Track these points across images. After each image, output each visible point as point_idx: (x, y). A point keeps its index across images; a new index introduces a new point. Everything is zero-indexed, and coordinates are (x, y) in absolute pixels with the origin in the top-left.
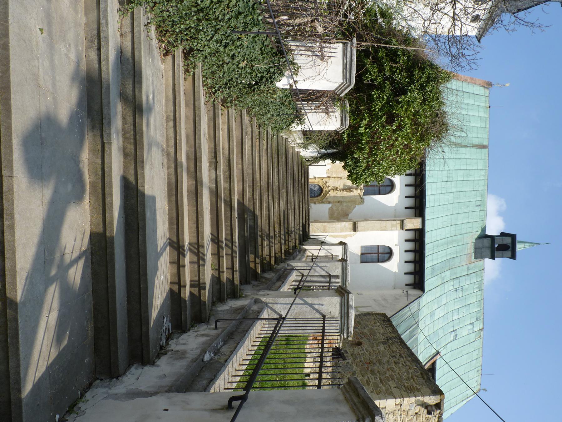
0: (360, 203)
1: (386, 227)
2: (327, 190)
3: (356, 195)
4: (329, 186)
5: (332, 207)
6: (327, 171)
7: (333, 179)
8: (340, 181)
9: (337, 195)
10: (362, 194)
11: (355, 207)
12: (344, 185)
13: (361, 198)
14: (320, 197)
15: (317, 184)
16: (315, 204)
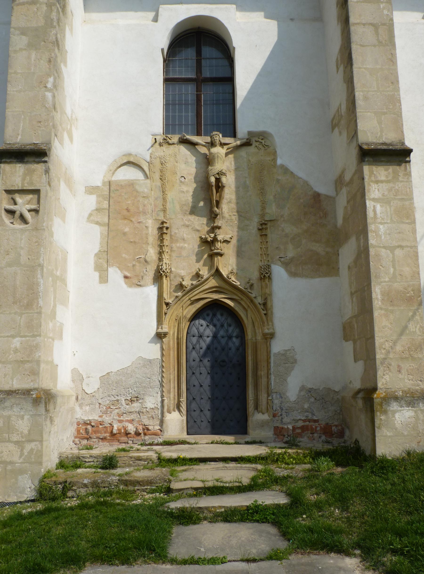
0: (266, 146)
1: (375, 27)
2: (213, 283)
3: (233, 167)
4: (198, 275)
5: (286, 265)
7: (166, 257)
8: (174, 230)
9: (234, 242)
10: (227, 140)
11: (285, 170)
12: (194, 211)
13: (247, 144)
15: (185, 325)
16: (272, 336)
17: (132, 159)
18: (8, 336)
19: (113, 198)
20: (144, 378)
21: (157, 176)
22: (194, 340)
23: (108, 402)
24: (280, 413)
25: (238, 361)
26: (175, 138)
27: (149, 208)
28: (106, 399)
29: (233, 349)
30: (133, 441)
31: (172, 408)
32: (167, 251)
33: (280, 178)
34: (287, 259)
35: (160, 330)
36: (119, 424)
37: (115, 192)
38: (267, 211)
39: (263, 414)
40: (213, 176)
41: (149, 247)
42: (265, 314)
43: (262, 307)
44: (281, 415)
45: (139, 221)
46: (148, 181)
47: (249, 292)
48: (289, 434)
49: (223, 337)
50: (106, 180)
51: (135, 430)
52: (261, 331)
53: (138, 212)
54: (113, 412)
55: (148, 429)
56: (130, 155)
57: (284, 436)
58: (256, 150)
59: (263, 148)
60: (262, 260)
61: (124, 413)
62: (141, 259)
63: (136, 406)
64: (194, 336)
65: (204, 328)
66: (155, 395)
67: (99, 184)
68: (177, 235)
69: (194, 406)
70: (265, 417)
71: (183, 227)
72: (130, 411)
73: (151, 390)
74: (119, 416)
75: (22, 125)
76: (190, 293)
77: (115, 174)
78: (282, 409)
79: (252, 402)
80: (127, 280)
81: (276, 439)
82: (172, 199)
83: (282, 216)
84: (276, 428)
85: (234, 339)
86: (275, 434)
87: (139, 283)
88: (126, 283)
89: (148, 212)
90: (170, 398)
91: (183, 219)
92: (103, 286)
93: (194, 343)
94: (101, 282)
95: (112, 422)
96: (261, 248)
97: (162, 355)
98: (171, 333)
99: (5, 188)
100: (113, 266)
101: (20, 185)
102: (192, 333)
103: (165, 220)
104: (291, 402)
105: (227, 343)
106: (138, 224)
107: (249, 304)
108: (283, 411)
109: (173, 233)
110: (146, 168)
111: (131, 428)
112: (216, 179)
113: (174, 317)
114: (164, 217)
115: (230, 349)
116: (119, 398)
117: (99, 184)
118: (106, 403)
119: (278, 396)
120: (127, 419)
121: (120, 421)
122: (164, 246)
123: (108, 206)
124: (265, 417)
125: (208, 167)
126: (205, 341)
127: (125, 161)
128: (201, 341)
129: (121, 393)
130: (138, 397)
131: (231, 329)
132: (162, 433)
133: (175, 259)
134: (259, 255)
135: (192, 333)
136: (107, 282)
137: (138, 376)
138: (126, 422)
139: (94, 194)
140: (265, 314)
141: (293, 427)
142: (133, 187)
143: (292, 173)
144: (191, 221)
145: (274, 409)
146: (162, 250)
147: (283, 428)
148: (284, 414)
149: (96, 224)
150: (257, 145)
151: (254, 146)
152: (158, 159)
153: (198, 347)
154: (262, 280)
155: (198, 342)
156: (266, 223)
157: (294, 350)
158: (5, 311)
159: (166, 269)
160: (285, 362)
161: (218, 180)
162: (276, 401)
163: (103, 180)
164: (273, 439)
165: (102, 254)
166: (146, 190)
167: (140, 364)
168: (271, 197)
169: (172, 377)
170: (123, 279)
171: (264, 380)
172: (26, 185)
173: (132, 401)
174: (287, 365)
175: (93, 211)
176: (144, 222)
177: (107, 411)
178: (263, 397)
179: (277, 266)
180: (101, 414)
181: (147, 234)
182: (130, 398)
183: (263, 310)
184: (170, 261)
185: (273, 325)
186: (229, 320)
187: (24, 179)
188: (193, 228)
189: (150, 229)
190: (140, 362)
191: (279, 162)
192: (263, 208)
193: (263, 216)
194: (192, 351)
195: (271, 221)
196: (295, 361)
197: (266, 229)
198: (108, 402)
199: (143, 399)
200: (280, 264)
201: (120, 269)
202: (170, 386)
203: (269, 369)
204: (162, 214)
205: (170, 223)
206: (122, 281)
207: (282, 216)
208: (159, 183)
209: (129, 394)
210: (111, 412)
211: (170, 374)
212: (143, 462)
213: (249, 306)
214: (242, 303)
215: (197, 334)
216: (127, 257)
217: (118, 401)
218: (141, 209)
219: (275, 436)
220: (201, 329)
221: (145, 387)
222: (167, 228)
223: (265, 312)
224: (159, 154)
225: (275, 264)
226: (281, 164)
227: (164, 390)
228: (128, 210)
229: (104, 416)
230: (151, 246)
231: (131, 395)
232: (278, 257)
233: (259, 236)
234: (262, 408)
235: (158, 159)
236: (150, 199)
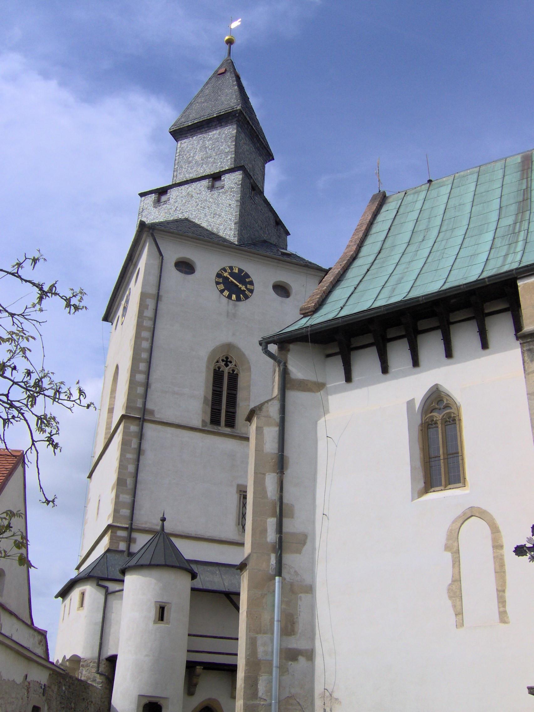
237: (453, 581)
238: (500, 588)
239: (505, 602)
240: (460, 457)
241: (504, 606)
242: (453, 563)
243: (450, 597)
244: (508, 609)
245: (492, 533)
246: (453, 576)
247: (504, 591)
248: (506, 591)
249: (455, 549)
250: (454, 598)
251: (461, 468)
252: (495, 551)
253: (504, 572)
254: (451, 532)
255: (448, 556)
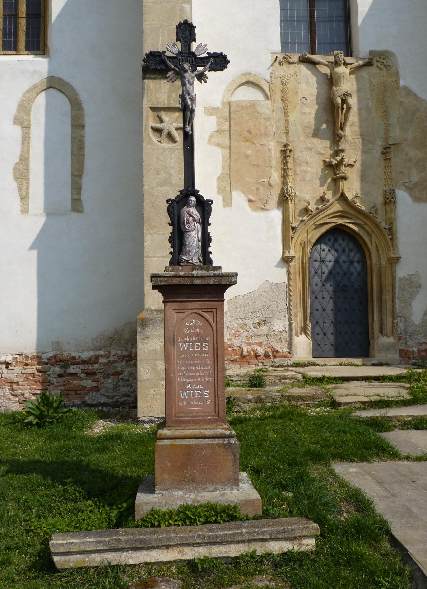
2: (337, 207)
3: (355, 88)
4: (322, 200)
5: (410, 189)
6: (255, 209)
7: (290, 181)
8: (297, 153)
9: (358, 166)
11: (408, 92)
12: (316, 134)
13: (369, 64)
14: (366, 239)
15: (308, 249)
16: (398, 259)
17: (251, 79)
18: (163, 256)
19: (234, 119)
20: (271, 302)
21: (278, 97)
22: (317, 264)
23: (236, 325)
24: (404, 337)
25: (360, 286)
26: (295, 58)
27: (271, 130)
28: (234, 323)
29: (355, 274)
30: (263, 363)
31: (299, 332)
32: (290, 174)
33: (403, 100)
34: (411, 184)
35: (287, 254)
36: (248, 347)
37: (235, 112)
38: (391, 134)
39: (388, 337)
40: (340, 96)
41: (272, 170)
42: (390, 239)
43: (388, 232)
44: (406, 338)
45: (262, 143)
46: (269, 102)
47: (375, 217)
48: (415, 357)
49: (344, 262)
50: (226, 100)
51: (264, 352)
52: (385, 256)
53: (260, 134)
54: (242, 335)
55: (277, 352)
56: (249, 74)
57: (410, 358)
58: (377, 71)
59: (384, 69)
60: (387, 184)
61: (253, 336)
62: (265, 183)
63: (264, 329)
64: (316, 261)
65: (325, 254)
66: (282, 319)
67: (219, 104)
68: (301, 158)
69: (317, 329)
70: (391, 340)
71: (306, 150)
72: (259, 334)
73: (278, 313)
74: (248, 338)
75: (161, 39)
76: (315, 217)
77: (234, 94)
78: (406, 333)
79: (377, 325)
80: (251, 204)
81: (402, 362)
82: (294, 121)
83: (406, 140)
84: (401, 351)
85: (356, 264)
86: (401, 356)
87: (263, 207)
88: (250, 207)
89: (270, 134)
90: (297, 322)
91: (305, 142)
92: (228, 210)
93: (317, 268)
94: (224, 206)
95: (241, 345)
96: (385, 172)
97: (289, 279)
98: (297, 257)
99: (150, 106)
100: (236, 189)
101: (166, 102)
102: (314, 258)
103: (288, 143)
104: (415, 325)
105: (348, 268)
106: (261, 146)
107: (373, 228)
108: (408, 335)
109: (296, 157)
110: (266, 88)
111: (261, 351)
112: (342, 100)
113: (299, 242)
114: (287, 139)
115: (352, 274)
116: (247, 321)
117: (219, 104)
118: (235, 327)
119: (403, 320)
120: (255, 341)
121: (249, 344)
122: (288, 169)
123: (228, 128)
124: (391, 340)
125: (331, 88)
126: (327, 266)
127: (245, 81)
128: (323, 266)
129: (249, 317)
130: (266, 321)
131: (352, 254)
132: (291, 355)
133: (299, 183)
134: (383, 179)
135: (314, 258)
136: (231, 205)
137: (264, 299)
138: (254, 345)
139: (214, 115)
140: (390, 239)
141: (418, 350)
142: (254, 108)
143: (415, 95)
144: (314, 144)
145: (399, 332)
146: (286, 173)
147: (408, 351)
148: (409, 338)
149: (217, 146)
150: (379, 65)
151: (375, 66)
152: (279, 79)
153: (320, 272)
154: (387, 205)
155: (320, 266)
156: (390, 146)
157: (418, 275)
158: (158, 231)
159: (292, 193)
160: (410, 287)
161: (344, 101)
162: (401, 325)
163: (222, 101)
164: (399, 361)
165: (225, 177)
166: (267, 111)
167: (267, 287)
168: (395, 120)
169: (298, 301)
170: (247, 203)
171: (389, 304)
172: (172, 102)
173: (259, 324)
174: (411, 289)
175: (213, 132)
176: (266, 144)
177: (235, 334)
178: (388, 321)
179: (401, 191)
180: (230, 337)
181: (270, 157)
182: (258, 321)
183: (389, 235)
184: (294, 185)
185: (397, 250)
186: (351, 245)
187: (169, 97)
188: (316, 151)
189: (273, 152)
190: (267, 286)
191: (402, 83)
192: (387, 131)
193: (386, 139)
194: (314, 276)
195: (394, 144)
196: (420, 286)
197: (390, 152)
198: (236, 325)
199: (270, 322)
200: (404, 188)
201: (243, 193)
202: (297, 310)
203: (394, 294)
204: (284, 136)
205: (293, 146)
206: (246, 205)
207: (406, 140)
208: (280, 104)
209: (256, 318)
210: (239, 336)
211: (297, 298)
212: (289, 381)
213: (373, 231)
214: (367, 227)
215: (319, 259)
216: (250, 180)
217: (245, 324)
218: (263, 131)
219: (400, 359)
220: (323, 254)
221: (272, 310)
222: (290, 151)
223: (391, 237)
224: (280, 74)
225: (399, 189)
226: (404, 86)
227: (292, 313)
228: (249, 132)
229: (233, 339)
230: (274, 169)
231: (258, 318)
232: (402, 182)
233: (382, 160)
234: (387, 332)
235: (279, 78)
236: (272, 121)
237: (21, 160)
238: (76, 173)
239: (80, 188)
240: (41, 18)
241: (79, 193)
242: (22, 139)
243: (16, 178)
244: (84, 196)
245: (72, 110)
246: (21, 155)
247: (80, 177)
248: (83, 177)
249: (26, 123)
250: (20, 180)
251: (42, 32)
252: (74, 130)
253: (83, 156)
254: (23, 103)
255: (17, 131)
